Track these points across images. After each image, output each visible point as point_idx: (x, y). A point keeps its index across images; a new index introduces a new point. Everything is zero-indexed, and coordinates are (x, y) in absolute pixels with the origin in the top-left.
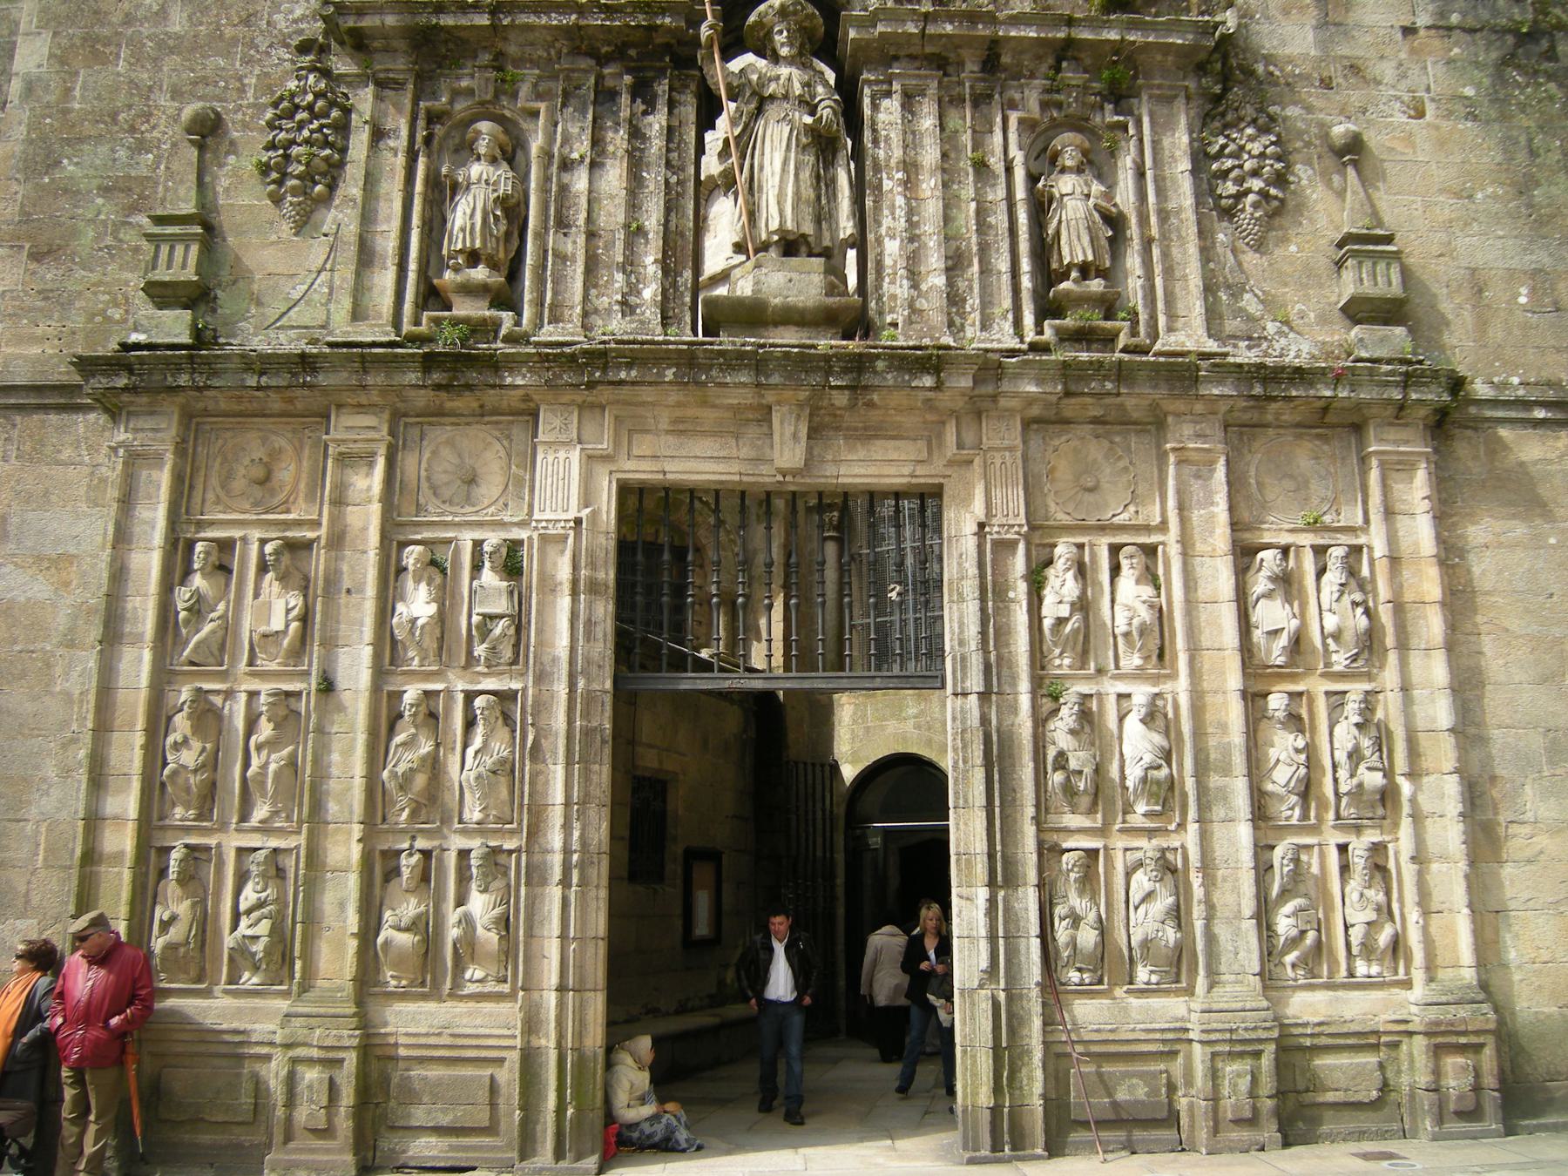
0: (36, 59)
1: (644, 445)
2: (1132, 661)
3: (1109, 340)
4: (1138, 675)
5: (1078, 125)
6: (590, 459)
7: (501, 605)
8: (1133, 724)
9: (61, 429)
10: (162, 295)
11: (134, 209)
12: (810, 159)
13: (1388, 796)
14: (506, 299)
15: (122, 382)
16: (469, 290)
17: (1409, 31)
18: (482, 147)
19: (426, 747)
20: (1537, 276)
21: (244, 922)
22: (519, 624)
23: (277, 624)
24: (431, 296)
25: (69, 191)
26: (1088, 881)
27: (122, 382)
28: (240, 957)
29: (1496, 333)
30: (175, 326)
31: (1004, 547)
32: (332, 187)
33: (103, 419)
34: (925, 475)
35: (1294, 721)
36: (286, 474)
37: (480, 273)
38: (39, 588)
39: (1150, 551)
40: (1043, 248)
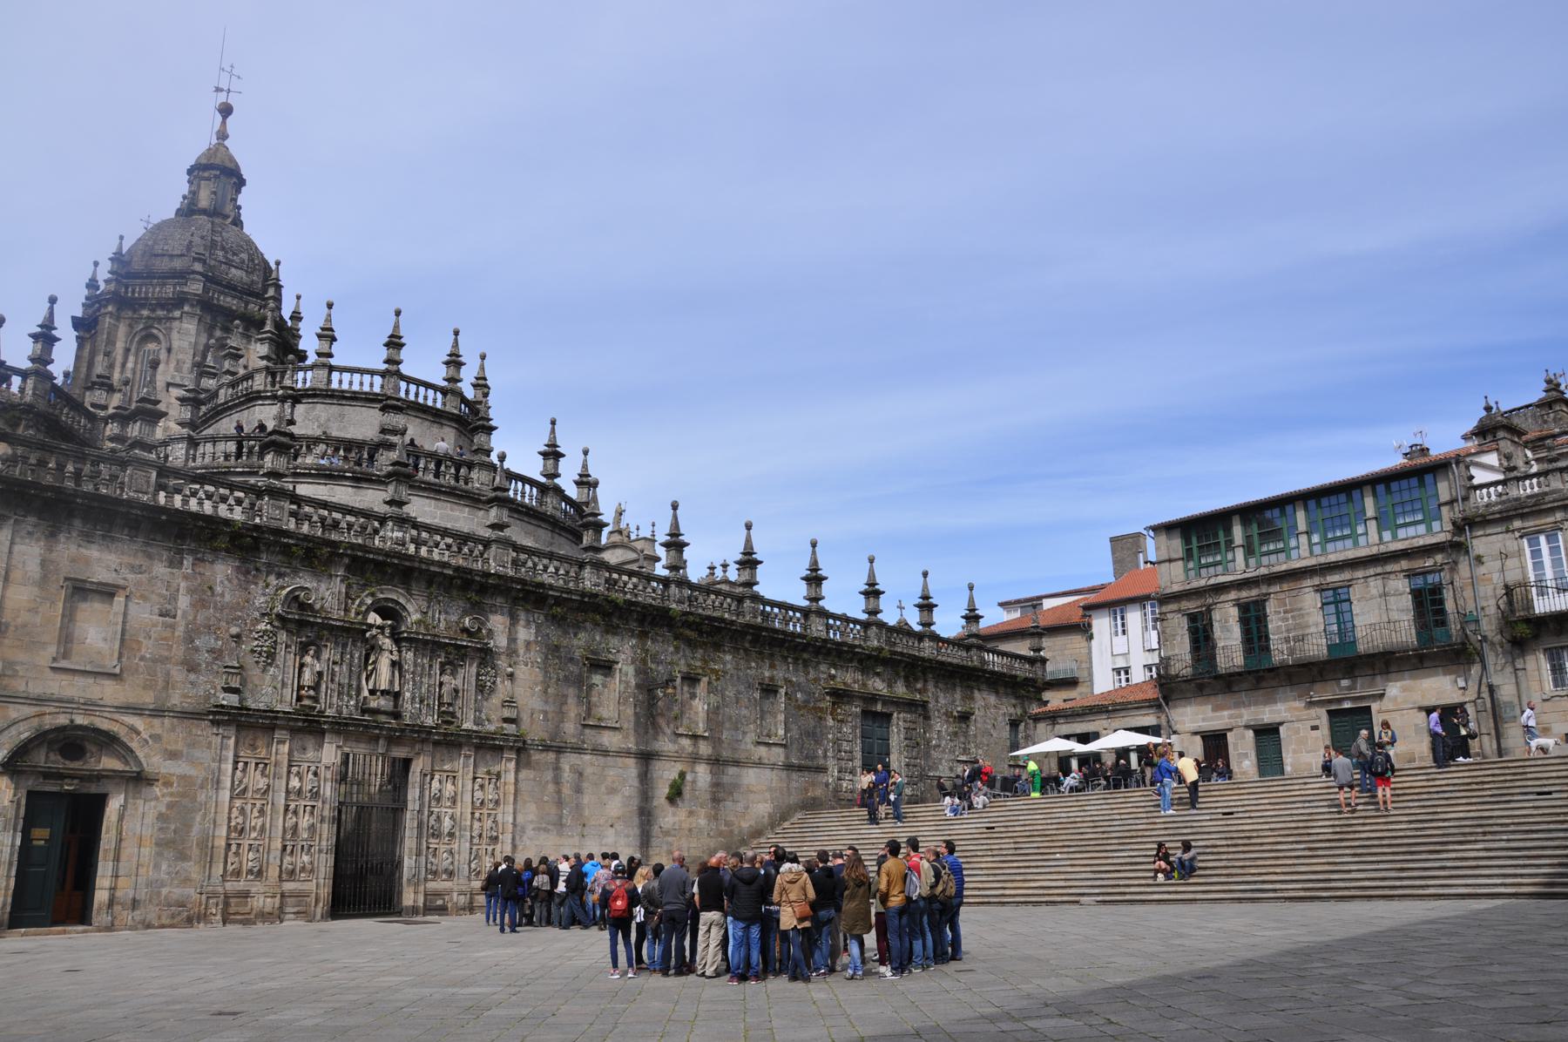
0: (185, 604)
1: (349, 744)
2: (449, 804)
3: (453, 723)
4: (450, 807)
5: (450, 663)
6: (338, 747)
7: (316, 784)
8: (447, 819)
9: (198, 726)
11: (216, 659)
14: (316, 699)
15: (226, 718)
16: (309, 697)
18: (312, 652)
19: (295, 819)
20: (545, 713)
21: (250, 863)
23: (260, 786)
24: (299, 699)
25: (197, 650)
26: (434, 856)
27: (226, 718)
28: (250, 872)
30: (233, 700)
31: (425, 775)
32: (273, 660)
33: (209, 724)
34: (410, 756)
35: (480, 820)
36: (259, 743)
37: (312, 693)
38: (193, 772)
39: (454, 777)
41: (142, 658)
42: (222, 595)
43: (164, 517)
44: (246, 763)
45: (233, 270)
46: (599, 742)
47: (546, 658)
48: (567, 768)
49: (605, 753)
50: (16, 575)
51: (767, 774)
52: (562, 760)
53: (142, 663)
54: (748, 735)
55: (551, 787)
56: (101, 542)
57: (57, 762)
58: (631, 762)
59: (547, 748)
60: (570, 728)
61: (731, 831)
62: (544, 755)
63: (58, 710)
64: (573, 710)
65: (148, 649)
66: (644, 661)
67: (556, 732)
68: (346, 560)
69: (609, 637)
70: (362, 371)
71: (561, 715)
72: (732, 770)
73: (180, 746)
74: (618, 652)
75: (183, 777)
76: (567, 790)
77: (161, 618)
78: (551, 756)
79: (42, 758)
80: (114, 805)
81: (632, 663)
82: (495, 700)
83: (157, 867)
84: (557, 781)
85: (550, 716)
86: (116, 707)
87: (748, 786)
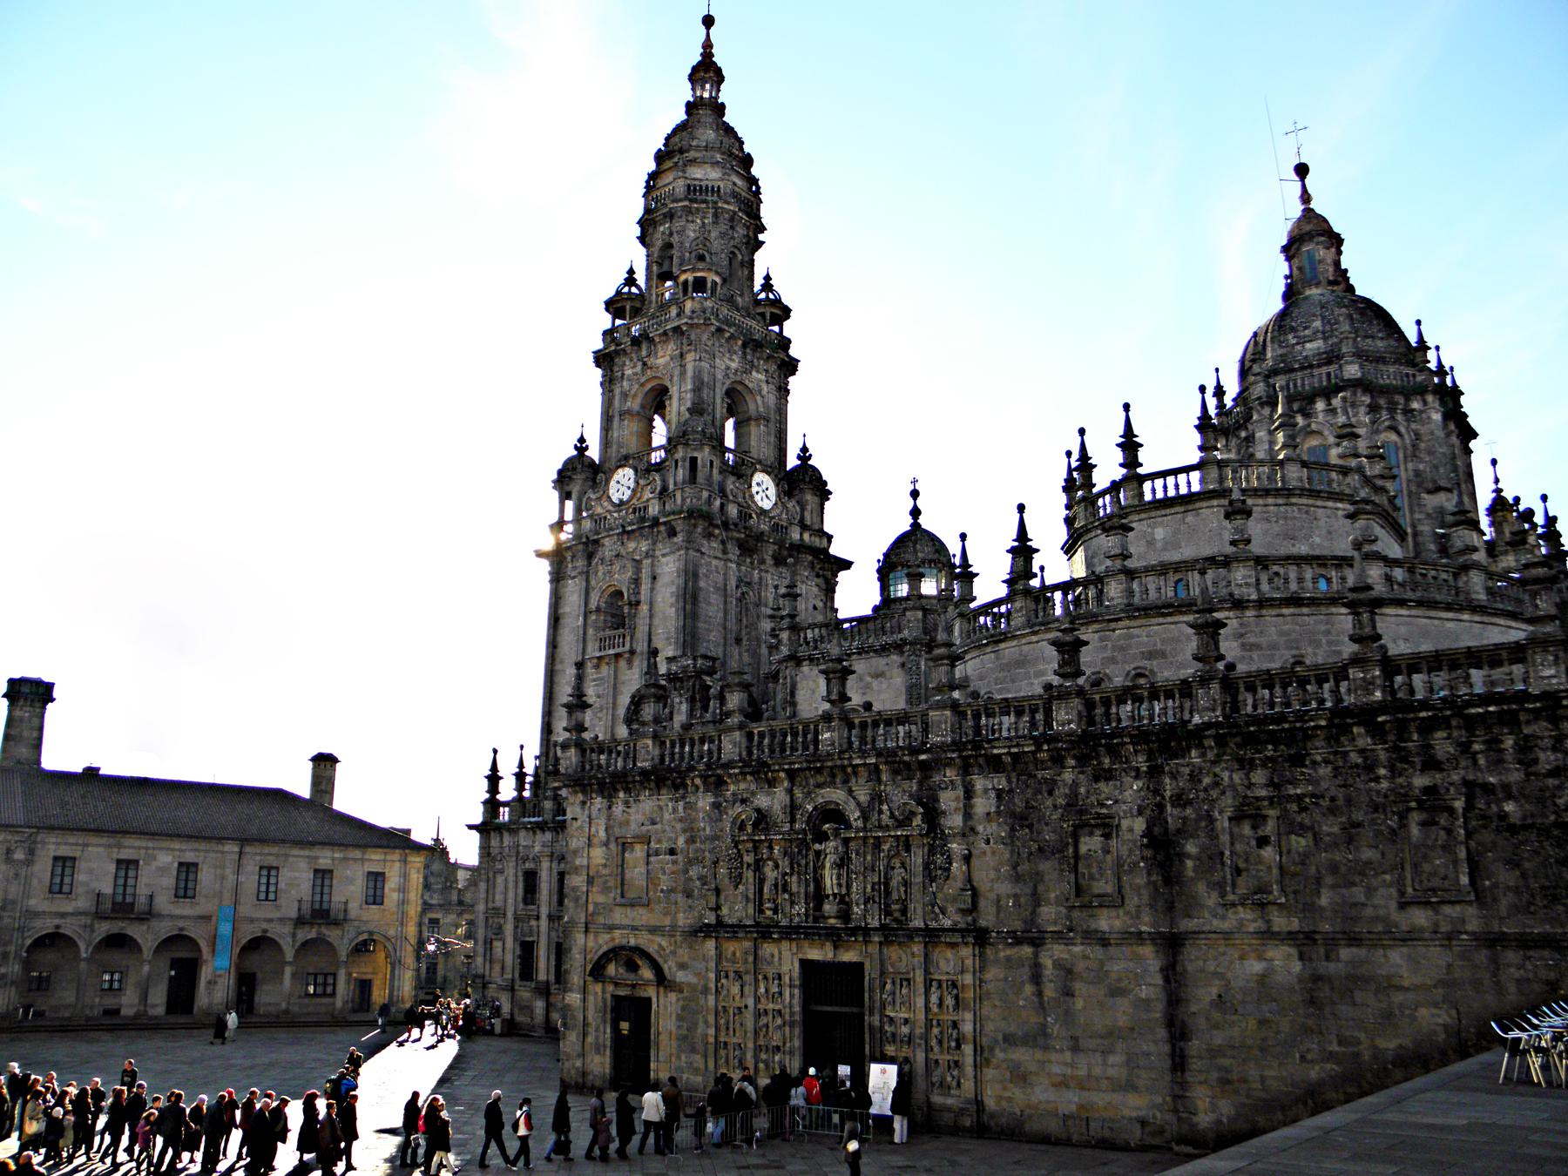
10: (711, 909)
11: (704, 884)
12: (835, 872)
13: (958, 1047)
17: (988, 814)
20: (1016, 897)
22: (780, 994)
29: (1002, 915)
38: (694, 980)
40: (888, 893)
41: (662, 891)
42: (704, 829)
44: (727, 972)
45: (1308, 345)
46: (1093, 926)
47: (1013, 829)
48: (1048, 963)
49: (1104, 942)
50: (595, 841)
51: (1436, 958)
52: (1041, 955)
54: (1382, 891)
55: (1029, 989)
58: (1147, 951)
59: (1018, 942)
60: (1050, 914)
61: (1357, 1055)
62: (1015, 950)
64: (1056, 886)
66: (1161, 807)
67: (1031, 921)
68: (782, 775)
69: (1102, 785)
70: (1175, 472)
71: (1037, 900)
72: (1345, 953)
73: (686, 959)
74: (1116, 802)
75: (689, 985)
76: (1050, 991)
78: (1027, 950)
81: (1140, 813)
82: (952, 888)
83: (679, 1058)
84: (1037, 979)
85: (1022, 900)
87: (1389, 977)
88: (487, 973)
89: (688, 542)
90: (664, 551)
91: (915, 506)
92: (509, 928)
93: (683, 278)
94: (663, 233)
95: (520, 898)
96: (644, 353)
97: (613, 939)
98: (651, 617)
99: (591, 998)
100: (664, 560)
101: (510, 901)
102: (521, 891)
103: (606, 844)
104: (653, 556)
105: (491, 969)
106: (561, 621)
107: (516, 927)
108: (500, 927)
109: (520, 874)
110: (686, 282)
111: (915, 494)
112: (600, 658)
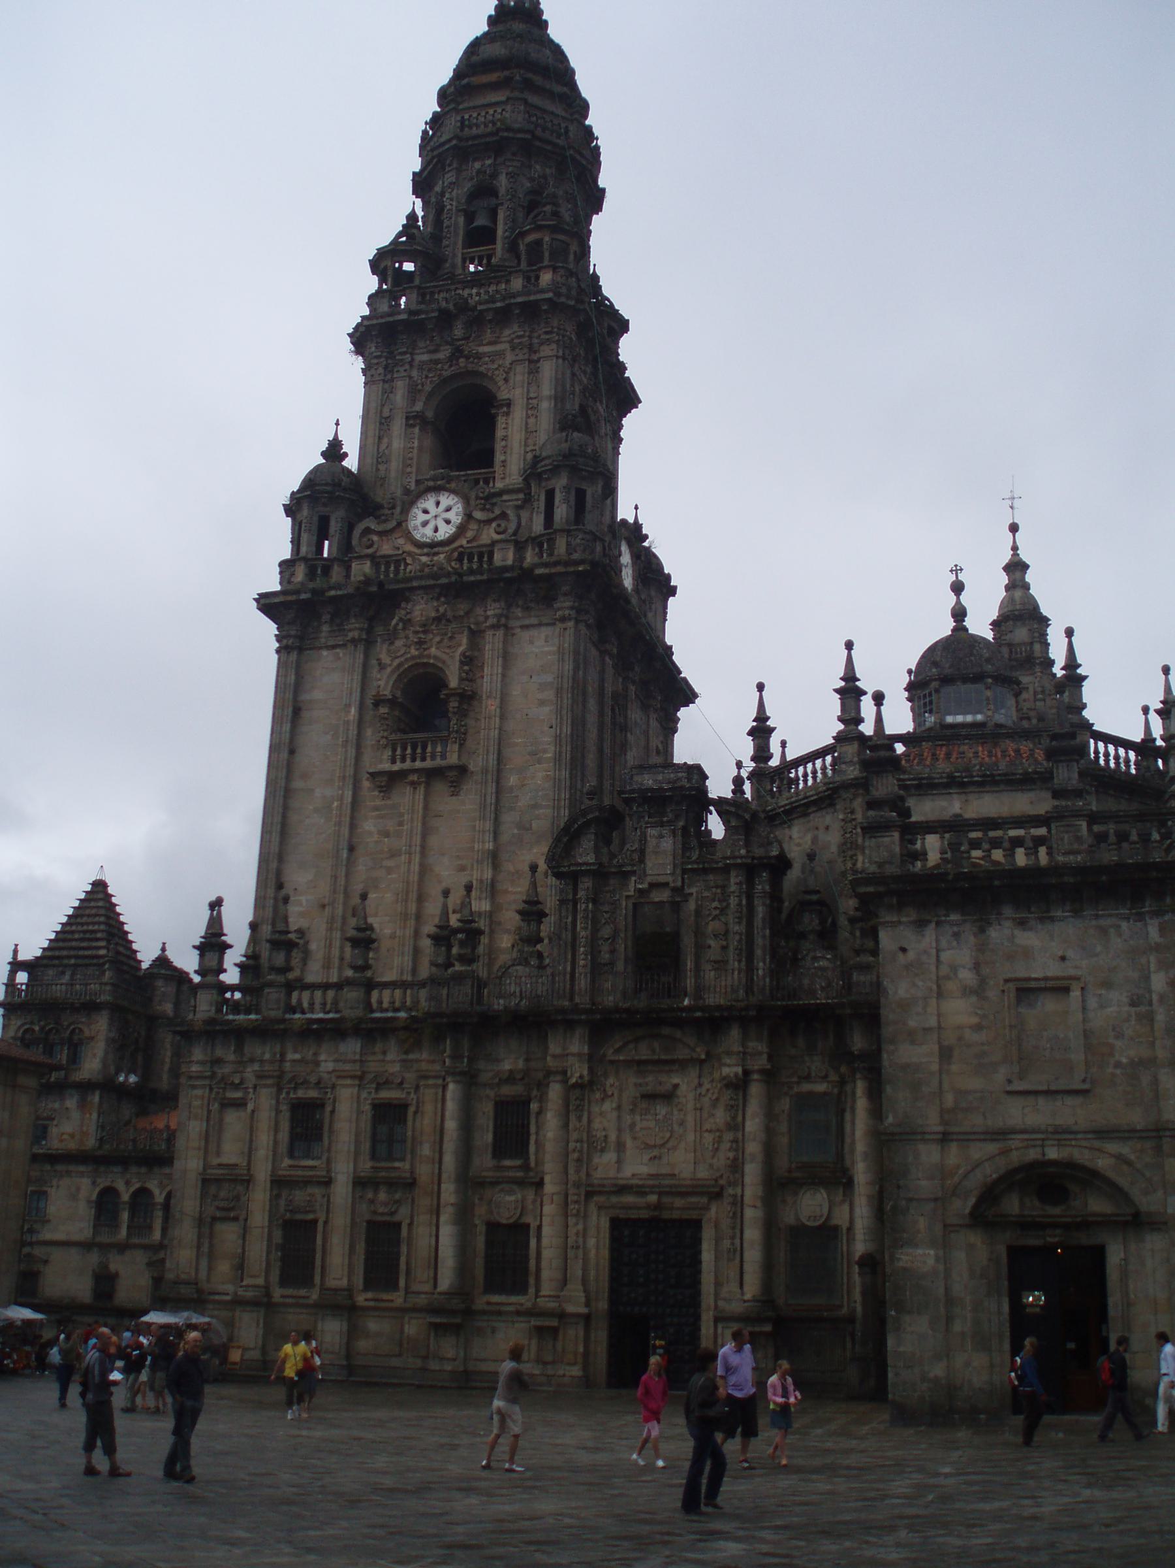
41: (1118, 1065)
43: (1104, 878)
50: (951, 986)
53: (1118, 1071)
56: (1040, 926)
57: (1034, 1208)
63: (1026, 1143)
65: (1125, 1053)
77: (1133, 1009)
79: (1012, 1205)
80: (1115, 1256)
86: (1094, 1132)
88: (203, 1274)
89: (579, 611)
90: (527, 622)
91: (958, 602)
92: (259, 1199)
93: (530, 238)
94: (479, 172)
95: (283, 1147)
96: (458, 332)
97: (1005, 1152)
98: (503, 717)
99: (960, 1256)
100: (525, 635)
101: (262, 1153)
102: (284, 1136)
103: (978, 991)
104: (506, 627)
105: (210, 1269)
106: (305, 714)
107: (275, 1198)
108: (237, 1198)
109: (284, 1107)
110: (538, 243)
111: (958, 588)
112: (400, 775)
